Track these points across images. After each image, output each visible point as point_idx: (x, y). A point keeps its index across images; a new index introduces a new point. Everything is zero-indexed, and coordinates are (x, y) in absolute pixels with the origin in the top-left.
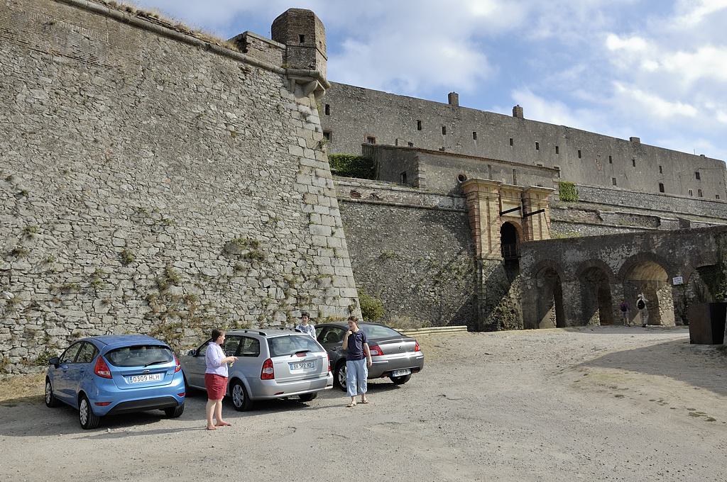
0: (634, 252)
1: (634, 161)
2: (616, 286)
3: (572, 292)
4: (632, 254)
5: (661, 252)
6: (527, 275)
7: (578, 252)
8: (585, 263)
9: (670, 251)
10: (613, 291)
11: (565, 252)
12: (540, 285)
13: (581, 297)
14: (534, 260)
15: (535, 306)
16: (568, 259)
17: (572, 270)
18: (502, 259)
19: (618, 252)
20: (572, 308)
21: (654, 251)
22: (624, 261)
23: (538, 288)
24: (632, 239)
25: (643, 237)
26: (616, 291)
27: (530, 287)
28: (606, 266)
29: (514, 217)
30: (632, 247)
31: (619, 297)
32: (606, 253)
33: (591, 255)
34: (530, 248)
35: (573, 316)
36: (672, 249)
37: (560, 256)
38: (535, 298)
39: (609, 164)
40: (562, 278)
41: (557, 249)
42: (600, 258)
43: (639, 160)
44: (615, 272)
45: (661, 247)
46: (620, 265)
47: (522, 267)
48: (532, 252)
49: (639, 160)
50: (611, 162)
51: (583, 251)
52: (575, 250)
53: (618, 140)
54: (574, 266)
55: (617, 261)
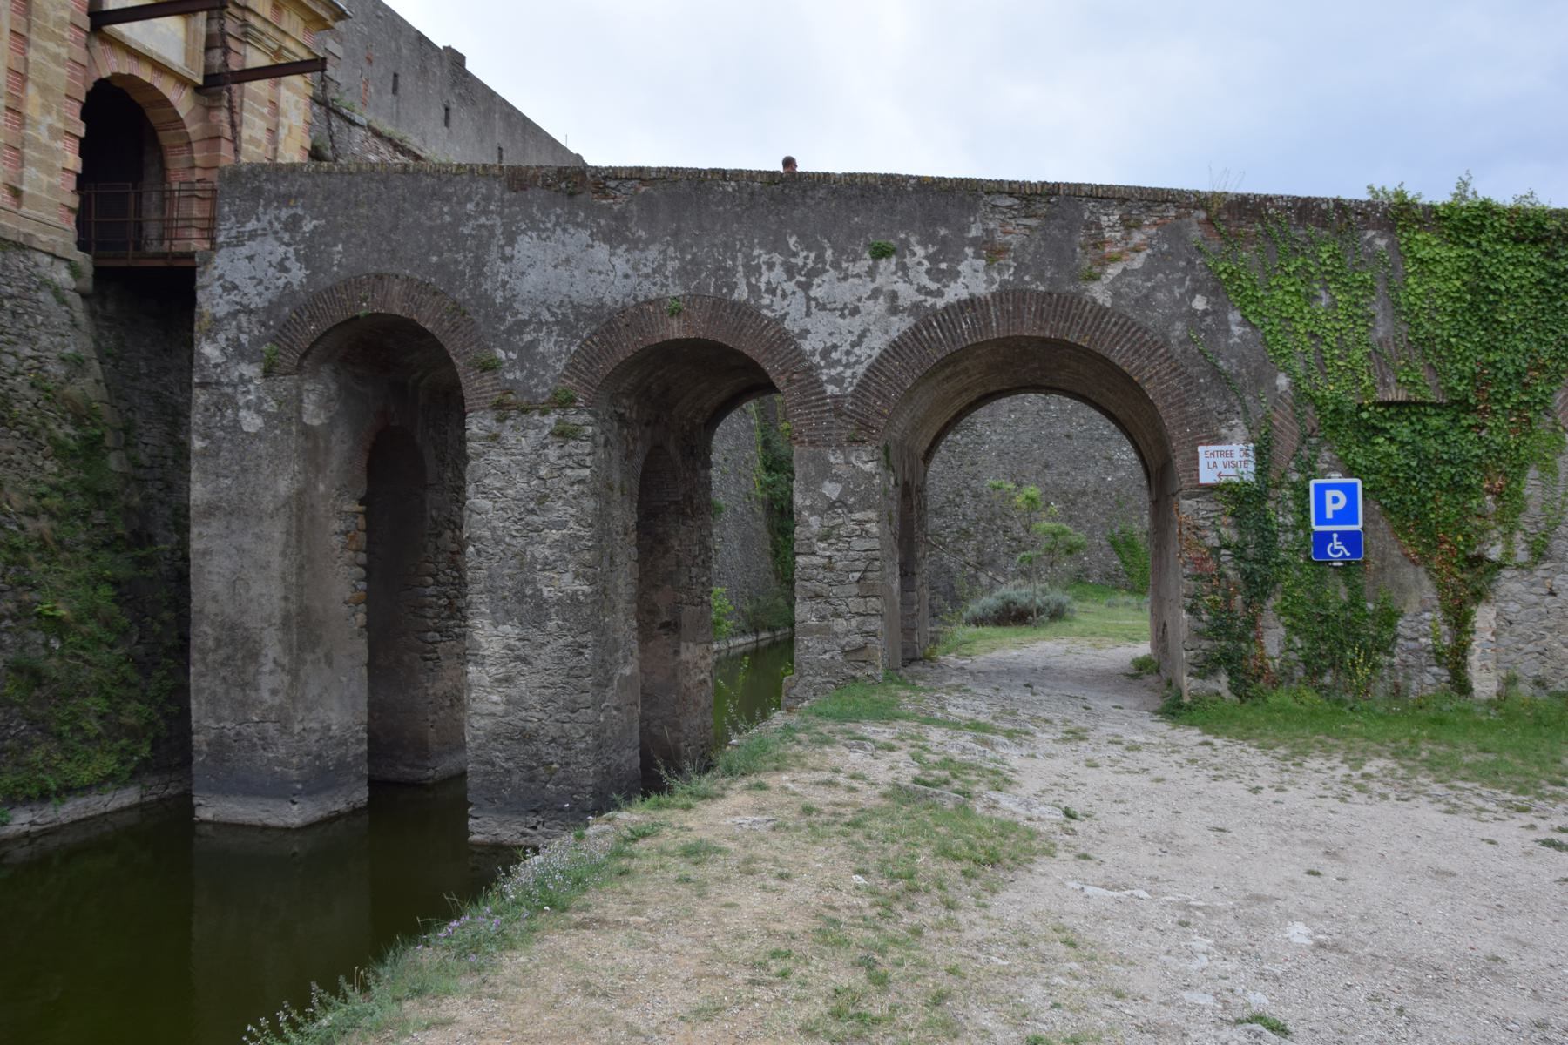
0: (973, 280)
1: (447, 110)
2: (836, 458)
3: (532, 471)
4: (955, 292)
5: (1144, 301)
6: (239, 352)
7: (601, 251)
8: (637, 313)
9: (1200, 303)
10: (812, 485)
11: (511, 240)
12: (314, 417)
13: (589, 504)
14: (298, 274)
15: (277, 530)
16: (531, 283)
17: (547, 346)
18: (83, 260)
19: (872, 273)
20: (526, 565)
21: (1100, 293)
22: (900, 325)
23: (307, 431)
24: (973, 209)
25: (1041, 207)
26: (832, 490)
27: (252, 422)
28: (785, 341)
29: (160, 67)
30: (959, 257)
31: (847, 523)
32: (791, 271)
33: (683, 273)
34: (285, 200)
35: (530, 609)
36: (1214, 292)
37: (479, 265)
38: (284, 486)
39: (390, 96)
40: (474, 386)
41: (459, 220)
42: (742, 293)
43: (460, 114)
44: (838, 381)
45: (1147, 273)
46: (876, 344)
47: (211, 301)
48: (293, 224)
49: (460, 114)
50: (395, 90)
51: (634, 244)
52: (584, 235)
53: (421, 38)
54: (566, 327)
55: (856, 323)
